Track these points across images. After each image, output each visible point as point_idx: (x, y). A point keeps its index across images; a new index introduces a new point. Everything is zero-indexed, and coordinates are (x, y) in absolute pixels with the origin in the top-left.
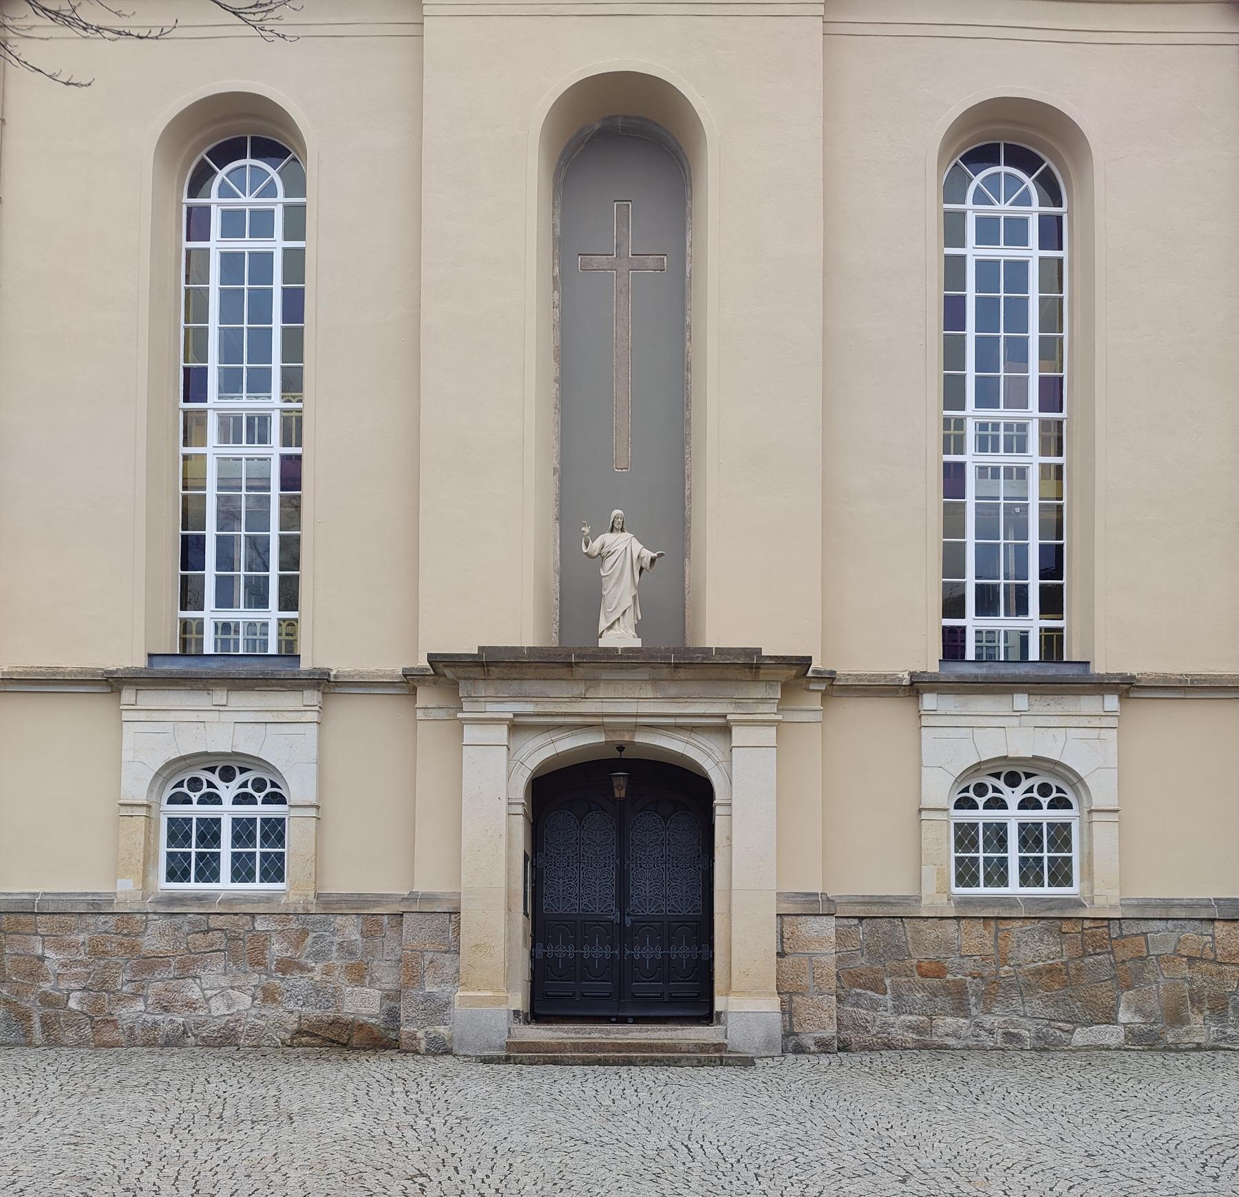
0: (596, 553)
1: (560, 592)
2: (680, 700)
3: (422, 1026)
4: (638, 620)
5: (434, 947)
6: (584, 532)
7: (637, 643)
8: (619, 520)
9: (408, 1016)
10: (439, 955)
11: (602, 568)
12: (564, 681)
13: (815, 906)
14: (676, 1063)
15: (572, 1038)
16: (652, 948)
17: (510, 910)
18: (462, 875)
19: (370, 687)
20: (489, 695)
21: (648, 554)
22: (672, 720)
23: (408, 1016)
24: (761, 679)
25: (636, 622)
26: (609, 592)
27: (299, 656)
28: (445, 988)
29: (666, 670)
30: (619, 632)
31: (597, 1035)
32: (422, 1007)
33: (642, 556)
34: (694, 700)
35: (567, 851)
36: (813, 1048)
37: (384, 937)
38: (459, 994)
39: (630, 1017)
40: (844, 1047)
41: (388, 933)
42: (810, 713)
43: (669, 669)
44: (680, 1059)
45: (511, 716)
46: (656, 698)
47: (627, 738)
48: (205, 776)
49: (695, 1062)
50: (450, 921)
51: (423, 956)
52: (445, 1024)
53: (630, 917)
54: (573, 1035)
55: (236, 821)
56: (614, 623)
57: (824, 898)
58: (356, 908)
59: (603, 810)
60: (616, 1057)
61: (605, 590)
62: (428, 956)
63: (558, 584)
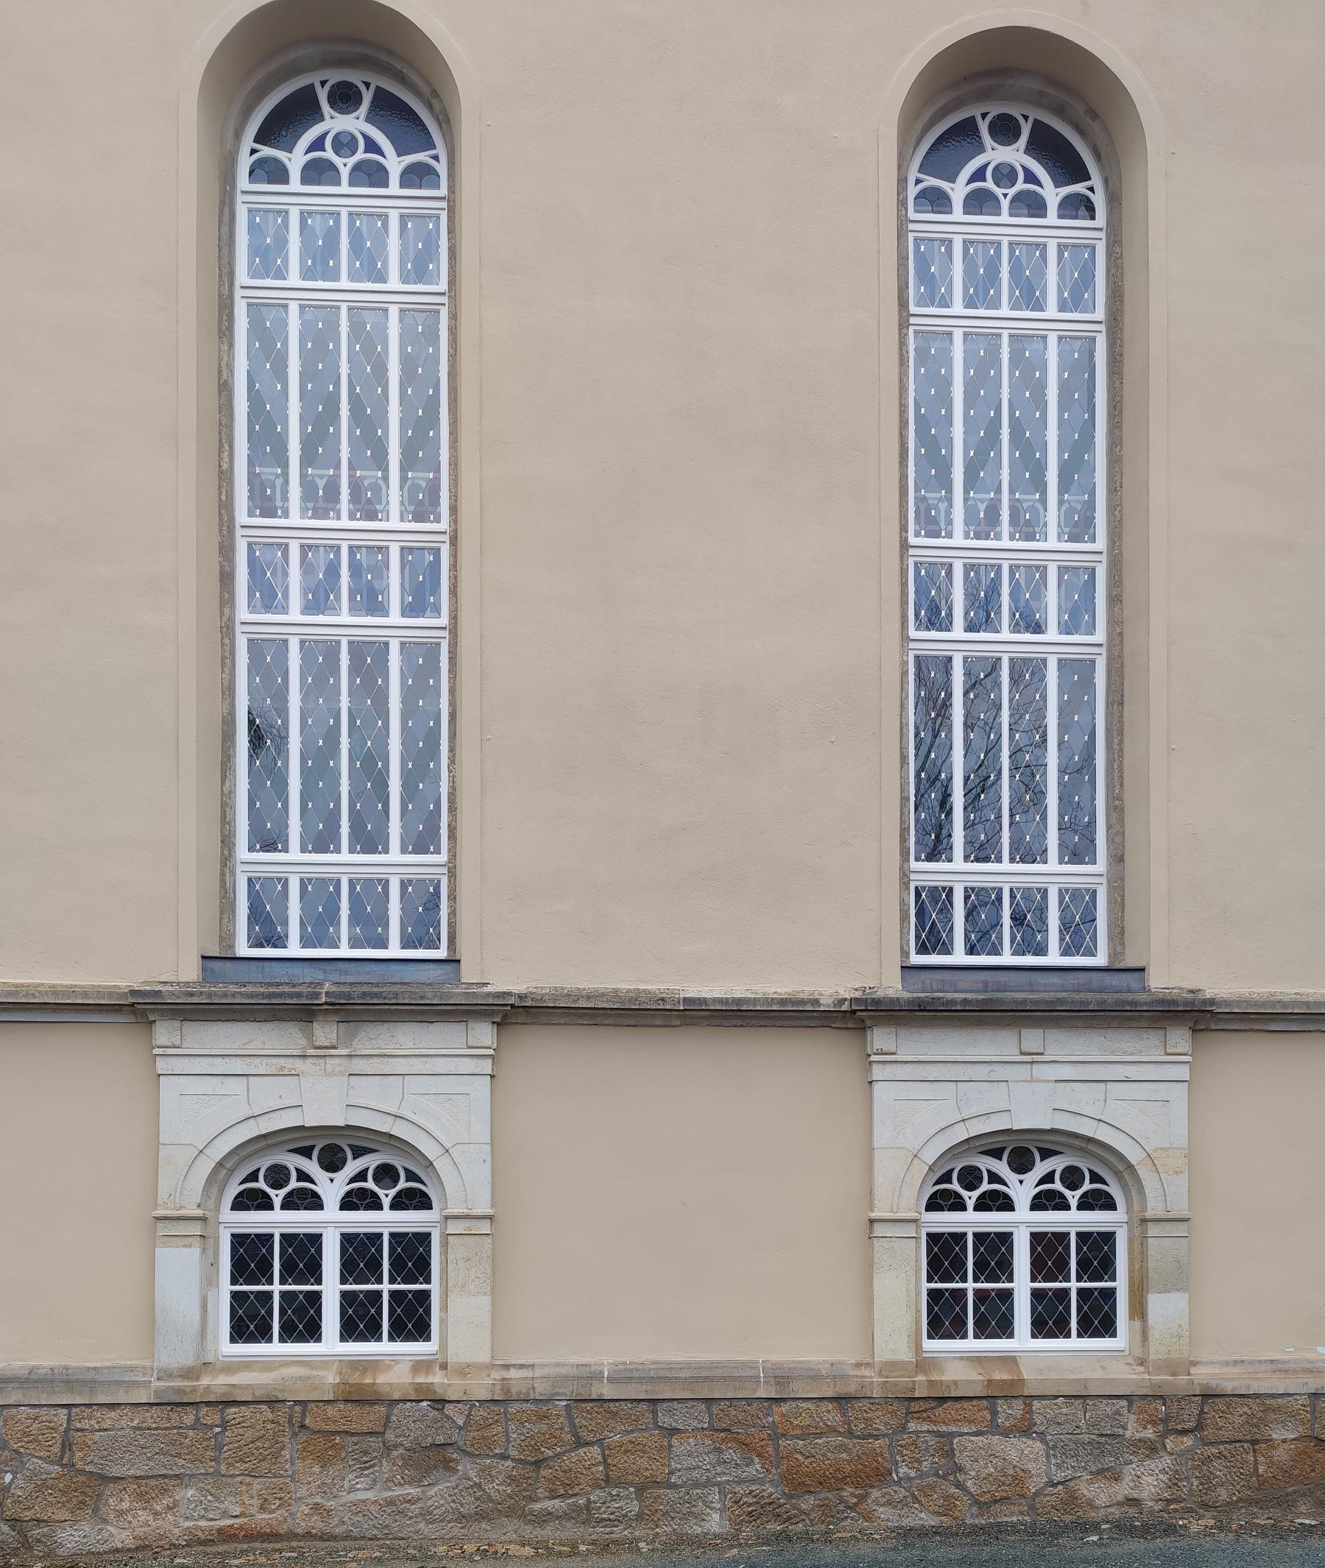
27: (459, 961)
48: (294, 1162)
55: (348, 1240)
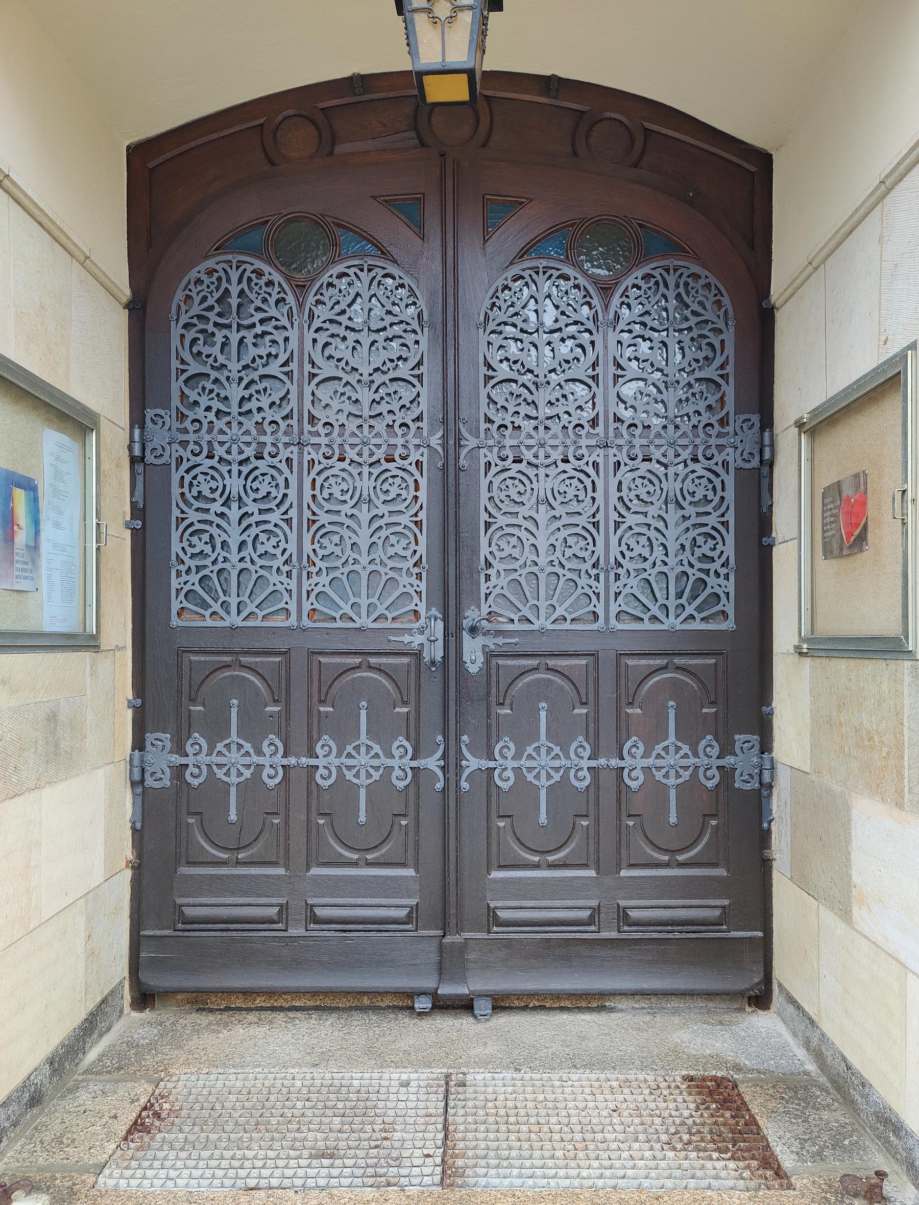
16: (557, 750)
35: (253, 405)
53: (480, 640)
59: (384, 254)
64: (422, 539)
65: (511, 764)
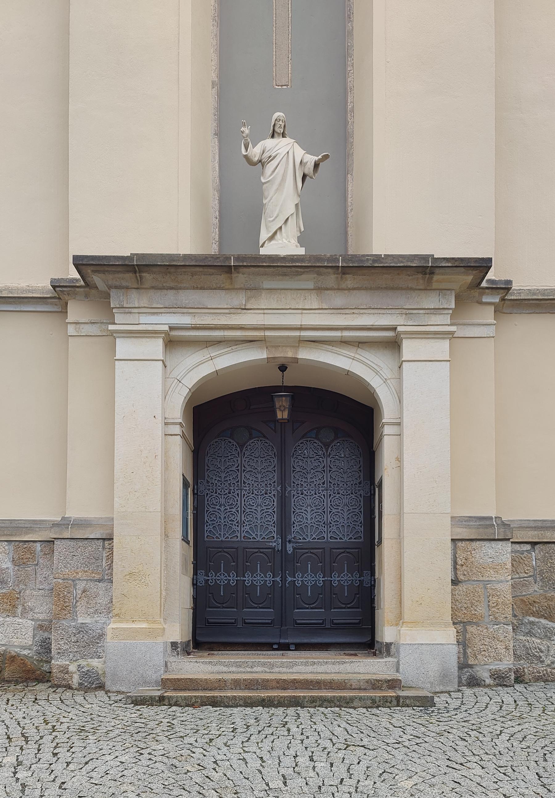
0: (256, 159)
1: (219, 212)
2: (347, 311)
3: (74, 659)
4: (301, 233)
5: (87, 576)
6: (243, 132)
7: (301, 251)
8: (281, 123)
9: (59, 649)
10: (91, 584)
11: (263, 176)
12: (224, 291)
13: (490, 530)
14: (347, 703)
15: (233, 672)
16: (313, 575)
17: (167, 536)
18: (116, 499)
19: (20, 303)
20: (143, 305)
21: (311, 159)
22: (338, 334)
23: (59, 649)
24: (434, 287)
25: (299, 235)
26: (270, 200)
28: (98, 619)
29: (333, 276)
30: (280, 242)
31: (259, 669)
32: (74, 639)
33: (305, 161)
34: (362, 311)
35: (228, 478)
36: (488, 681)
37: (37, 565)
38: (112, 625)
39: (292, 644)
40: (519, 679)
41: (41, 561)
42: (482, 327)
43: (336, 275)
44: (352, 699)
45: (166, 328)
46: (322, 309)
47: (290, 354)
49: (369, 703)
50: (104, 548)
51: (75, 586)
52: (99, 657)
53: (291, 545)
54: (234, 669)
56: (275, 233)
57: (499, 522)
58: (7, 535)
59: (264, 437)
60: (282, 697)
61: (266, 199)
62: (81, 586)
63: (217, 202)
64: (275, 516)
65: (300, 579)
